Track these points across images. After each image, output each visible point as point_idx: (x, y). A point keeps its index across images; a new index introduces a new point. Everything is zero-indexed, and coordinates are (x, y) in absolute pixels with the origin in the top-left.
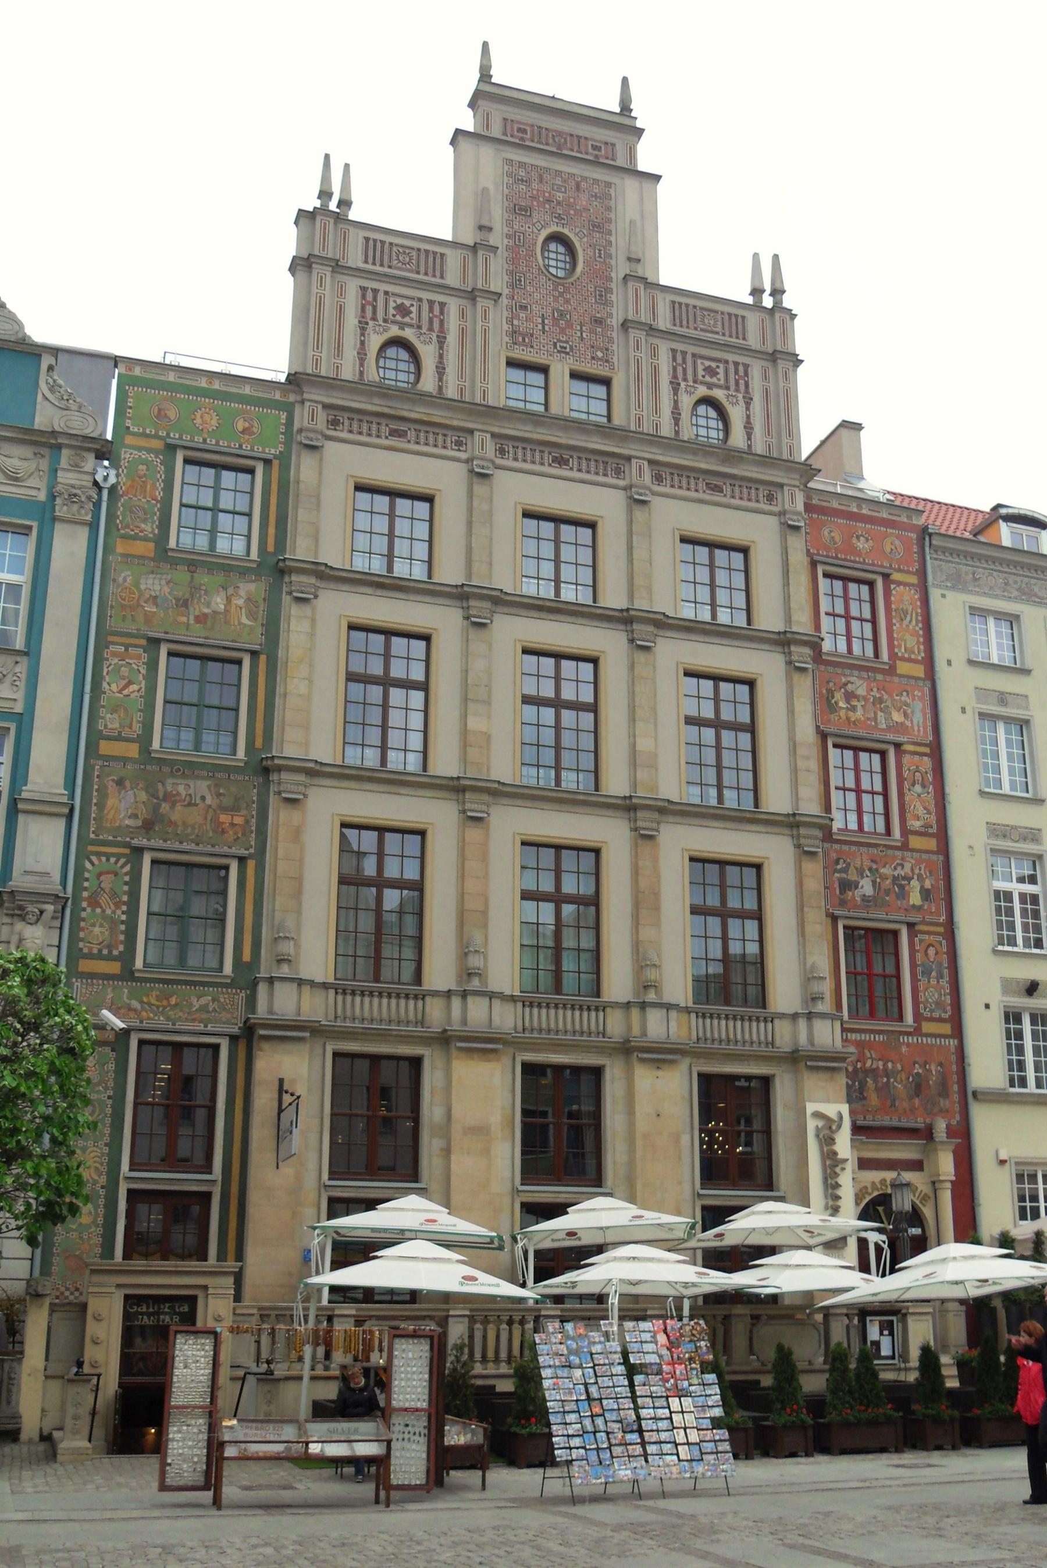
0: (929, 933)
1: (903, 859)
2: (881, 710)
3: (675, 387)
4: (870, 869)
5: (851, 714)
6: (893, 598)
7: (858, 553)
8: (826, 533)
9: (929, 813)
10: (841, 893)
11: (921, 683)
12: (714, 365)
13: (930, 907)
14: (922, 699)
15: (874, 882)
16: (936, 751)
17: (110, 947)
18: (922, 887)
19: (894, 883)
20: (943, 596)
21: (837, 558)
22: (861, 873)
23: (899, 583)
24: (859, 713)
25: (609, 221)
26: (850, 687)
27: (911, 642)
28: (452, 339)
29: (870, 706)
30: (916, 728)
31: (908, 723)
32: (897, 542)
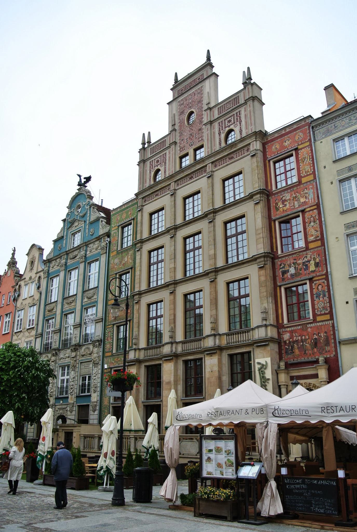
0: (318, 280)
1: (307, 254)
2: (296, 201)
3: (220, 134)
4: (294, 263)
5: (284, 208)
6: (299, 156)
7: (286, 147)
8: (274, 148)
9: (317, 231)
10: (283, 276)
11: (312, 182)
12: (230, 119)
13: (319, 269)
14: (312, 188)
15: (295, 268)
16: (318, 206)
17: (110, 349)
18: (315, 263)
19: (303, 265)
20: (321, 142)
21: (278, 154)
22: (290, 266)
23: (301, 149)
24: (288, 206)
25: (202, 97)
26: (284, 198)
27: (308, 168)
28: (167, 161)
29: (292, 201)
30: (310, 201)
31: (307, 200)
32: (300, 134)
